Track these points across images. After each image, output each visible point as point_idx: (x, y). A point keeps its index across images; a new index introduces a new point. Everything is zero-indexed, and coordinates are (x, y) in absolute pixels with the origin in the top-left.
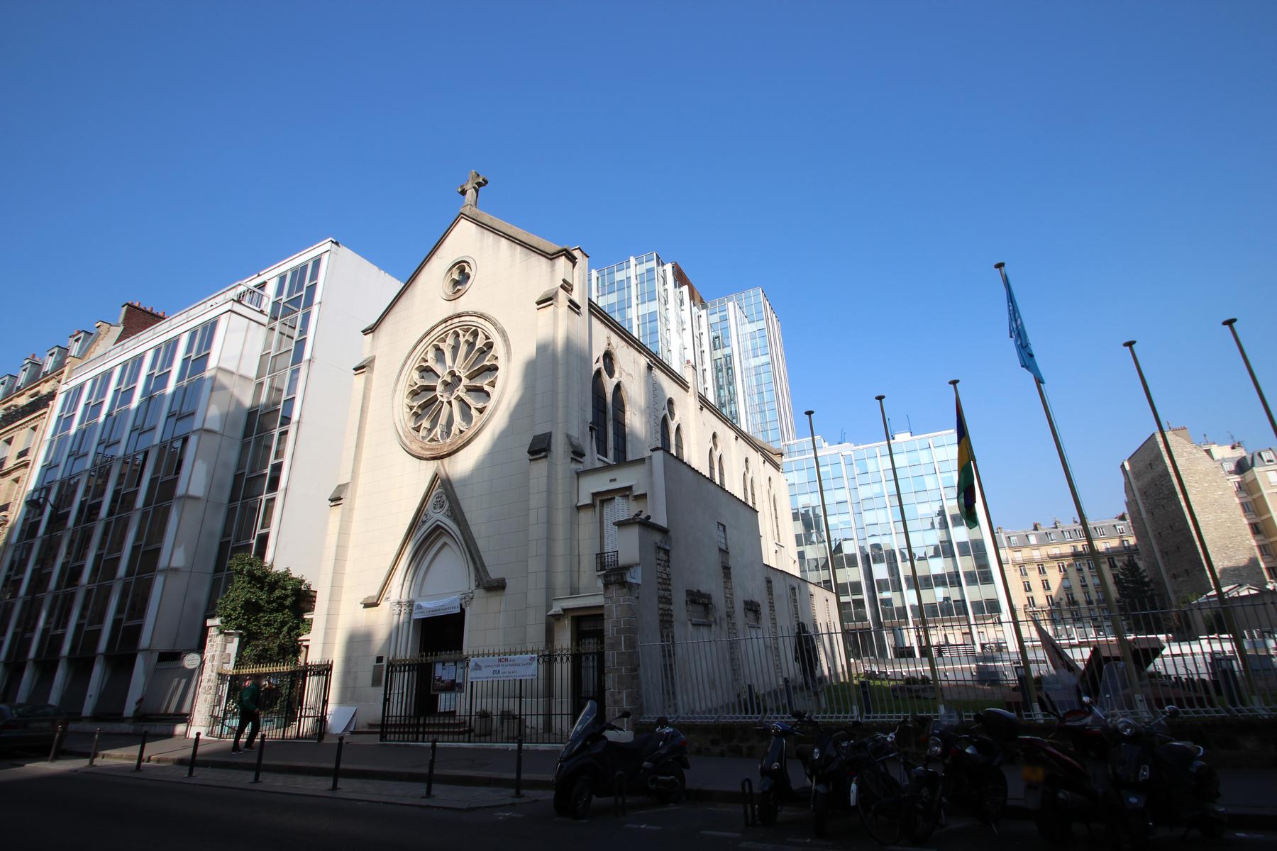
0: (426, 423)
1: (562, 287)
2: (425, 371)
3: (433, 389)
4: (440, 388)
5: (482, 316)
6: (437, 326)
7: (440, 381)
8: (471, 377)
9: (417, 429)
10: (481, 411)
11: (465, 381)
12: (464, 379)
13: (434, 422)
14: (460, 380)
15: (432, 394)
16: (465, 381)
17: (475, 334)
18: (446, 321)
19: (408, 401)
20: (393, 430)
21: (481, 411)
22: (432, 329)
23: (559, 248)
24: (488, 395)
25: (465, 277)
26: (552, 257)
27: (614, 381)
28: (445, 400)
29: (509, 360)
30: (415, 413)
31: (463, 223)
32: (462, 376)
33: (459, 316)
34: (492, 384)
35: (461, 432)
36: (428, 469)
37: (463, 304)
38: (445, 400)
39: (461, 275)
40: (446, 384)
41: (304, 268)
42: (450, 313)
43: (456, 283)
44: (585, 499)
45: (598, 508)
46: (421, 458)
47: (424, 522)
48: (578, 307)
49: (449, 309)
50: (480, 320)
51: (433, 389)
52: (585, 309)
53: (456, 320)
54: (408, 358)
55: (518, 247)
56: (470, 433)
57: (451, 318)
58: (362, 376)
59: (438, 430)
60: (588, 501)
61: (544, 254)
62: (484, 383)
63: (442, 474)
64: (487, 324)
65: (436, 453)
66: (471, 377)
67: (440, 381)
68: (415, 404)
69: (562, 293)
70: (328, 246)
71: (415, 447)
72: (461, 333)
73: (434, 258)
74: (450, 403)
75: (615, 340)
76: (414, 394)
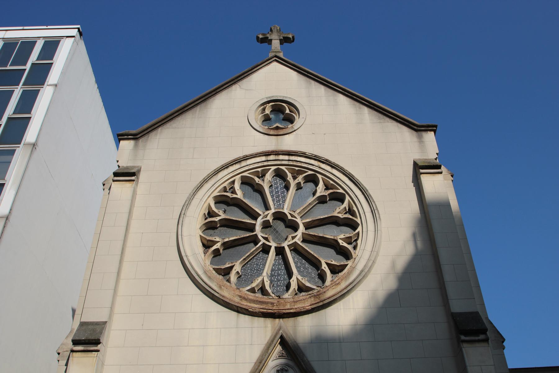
3: (252, 228)
4: (258, 228)
5: (327, 162)
7: (260, 220)
8: (308, 226)
9: (226, 273)
11: (302, 229)
13: (251, 270)
14: (294, 227)
16: (302, 229)
21: (335, 270)
22: (246, 158)
28: (273, 245)
30: (216, 253)
31: (275, 66)
32: (299, 220)
33: (289, 153)
34: (353, 241)
35: (301, 289)
36: (262, 331)
37: (288, 142)
38: (273, 245)
39: (279, 114)
40: (266, 225)
41: (29, 45)
43: (267, 119)
53: (286, 157)
54: (205, 181)
55: (366, 110)
57: (277, 153)
58: (128, 184)
62: (340, 235)
66: (308, 226)
70: (75, 32)
74: (280, 251)
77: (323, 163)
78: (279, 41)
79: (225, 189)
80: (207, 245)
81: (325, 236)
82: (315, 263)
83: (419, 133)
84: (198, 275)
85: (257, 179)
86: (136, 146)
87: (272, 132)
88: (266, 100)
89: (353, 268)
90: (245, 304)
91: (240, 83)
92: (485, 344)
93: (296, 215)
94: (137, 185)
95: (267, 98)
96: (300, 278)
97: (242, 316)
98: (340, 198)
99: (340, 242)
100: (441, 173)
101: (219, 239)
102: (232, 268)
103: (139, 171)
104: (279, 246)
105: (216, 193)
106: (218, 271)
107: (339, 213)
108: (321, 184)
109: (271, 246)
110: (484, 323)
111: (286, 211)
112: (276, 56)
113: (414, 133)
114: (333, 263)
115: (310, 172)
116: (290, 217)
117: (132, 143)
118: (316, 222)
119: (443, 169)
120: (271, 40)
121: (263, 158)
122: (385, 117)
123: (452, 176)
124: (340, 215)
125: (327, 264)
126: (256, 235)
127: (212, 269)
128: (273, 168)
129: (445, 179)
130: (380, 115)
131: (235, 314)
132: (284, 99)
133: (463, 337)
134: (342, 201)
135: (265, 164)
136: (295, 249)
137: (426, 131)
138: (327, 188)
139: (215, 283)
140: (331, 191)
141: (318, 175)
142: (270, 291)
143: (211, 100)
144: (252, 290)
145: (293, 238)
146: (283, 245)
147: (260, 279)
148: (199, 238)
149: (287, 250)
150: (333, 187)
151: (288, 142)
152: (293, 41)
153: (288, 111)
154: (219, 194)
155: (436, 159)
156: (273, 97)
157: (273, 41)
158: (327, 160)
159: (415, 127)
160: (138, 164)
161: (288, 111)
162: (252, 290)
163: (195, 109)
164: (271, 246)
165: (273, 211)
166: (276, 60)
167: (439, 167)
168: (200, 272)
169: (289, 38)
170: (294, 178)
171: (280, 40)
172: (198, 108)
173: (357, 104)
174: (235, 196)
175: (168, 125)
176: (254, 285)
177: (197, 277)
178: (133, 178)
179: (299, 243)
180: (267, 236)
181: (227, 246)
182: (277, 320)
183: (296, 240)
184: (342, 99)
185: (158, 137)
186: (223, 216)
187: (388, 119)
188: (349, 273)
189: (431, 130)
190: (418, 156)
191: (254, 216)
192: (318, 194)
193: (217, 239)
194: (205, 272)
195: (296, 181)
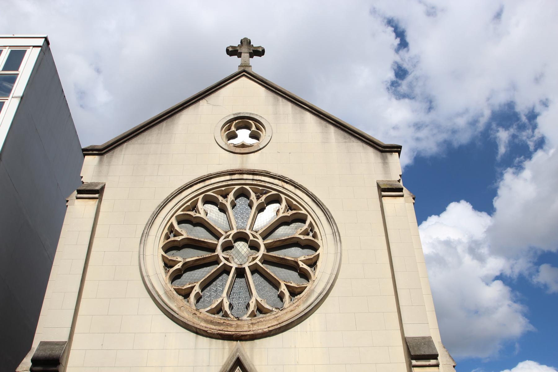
4: (219, 248)
7: (222, 240)
8: (269, 248)
18: (232, 173)
21: (294, 292)
24: (305, 276)
28: (234, 266)
33: (254, 173)
34: (313, 264)
35: (261, 310)
46: (198, 332)
49: (234, 162)
51: (211, 248)
53: (251, 177)
55: (332, 129)
56: (286, 316)
57: (241, 172)
65: (231, 330)
66: (269, 248)
67: (222, 240)
73: (203, 103)
77: (287, 183)
78: (248, 55)
79: (189, 209)
80: (168, 265)
81: (286, 258)
82: (275, 284)
83: (384, 154)
84: (159, 296)
85: (221, 199)
86: (101, 161)
87: (238, 150)
88: (232, 117)
89: (312, 291)
90: (203, 325)
91: (207, 98)
92: (436, 368)
93: (258, 236)
94: (100, 202)
95: (234, 114)
96: (259, 299)
97: (200, 338)
98: (302, 219)
99: (301, 263)
100: (402, 196)
101: (181, 258)
102: (192, 288)
103: (103, 188)
104: (240, 267)
106: (178, 291)
107: (300, 234)
108: (284, 203)
109: (232, 267)
110: (435, 348)
111: (248, 232)
112: (244, 71)
114: (292, 285)
115: (274, 192)
116: (251, 238)
117: (97, 158)
118: (278, 244)
119: (405, 191)
120: (241, 53)
121: (228, 177)
122: (350, 137)
123: (414, 199)
124: (302, 237)
125: (287, 286)
126: (218, 255)
127: (172, 289)
128: (237, 187)
129: (406, 202)
130: (346, 134)
131: (193, 335)
132: (251, 116)
133: (414, 362)
134: (304, 221)
135: (230, 183)
137: (391, 152)
138: (290, 207)
139: (176, 304)
140: (294, 212)
141: (281, 195)
142: (229, 312)
143: (177, 115)
144: (212, 312)
145: (254, 259)
146: (243, 266)
147: (219, 301)
148: (160, 258)
149: (248, 271)
150: (296, 208)
151: (253, 162)
152: (263, 54)
153: (254, 128)
154: (182, 213)
155: (399, 181)
156: (239, 113)
157: (243, 55)
158: (291, 181)
159: (380, 148)
160: (102, 180)
161: (254, 128)
162: (212, 312)
163: (161, 124)
164: (232, 267)
165: (235, 231)
166: (244, 75)
167: (401, 190)
168: (161, 293)
169: (259, 51)
170: (258, 198)
171: (250, 53)
172: (164, 124)
173: (324, 123)
174: (198, 215)
175: (134, 140)
176: (214, 306)
177: (157, 298)
178: (97, 196)
179: (260, 264)
180: (228, 257)
181: (190, 267)
182: (235, 342)
183: (257, 261)
184: (309, 117)
185: (123, 153)
186: (185, 236)
187: (353, 139)
188: (309, 295)
190: (381, 177)
191: (217, 236)
192: (281, 215)
193: (179, 259)
194: (166, 293)
195: (260, 201)
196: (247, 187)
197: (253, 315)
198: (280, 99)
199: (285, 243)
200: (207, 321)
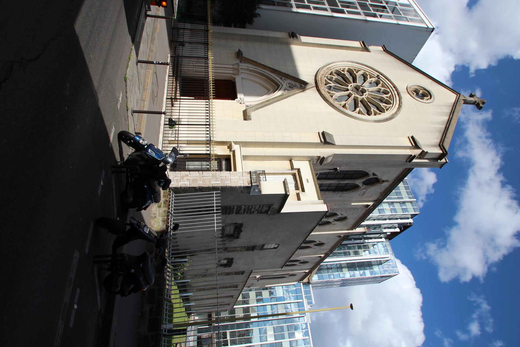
0: (335, 77)
1: (423, 151)
2: (365, 77)
5: (400, 106)
6: (391, 83)
10: (344, 106)
12: (362, 97)
13: (336, 81)
15: (351, 79)
17: (387, 102)
19: (347, 68)
20: (331, 62)
21: (344, 106)
23: (447, 150)
25: (423, 96)
26: (441, 145)
27: (361, 185)
29: (376, 121)
32: (364, 96)
35: (332, 96)
37: (406, 98)
42: (400, 90)
44: (297, 164)
45: (291, 172)
46: (316, 76)
47: (281, 78)
48: (410, 161)
49: (402, 88)
50: (397, 106)
51: (355, 80)
52: (408, 166)
55: (444, 126)
56: (331, 100)
59: (332, 84)
60: (295, 167)
61: (442, 140)
63: (308, 87)
64: (395, 109)
68: (346, 73)
69: (419, 151)
71: (322, 72)
72: (389, 95)
74: (348, 90)
75: (385, 185)
76: (350, 72)
105: (367, 73)
106: (332, 72)
111: (367, 93)
113: (438, 144)
118: (365, 104)
124: (372, 110)
136: (349, 96)
137: (441, 149)
173: (445, 123)
179: (353, 96)
189: (443, 151)
196: (390, 93)
197: (329, 93)
198: (451, 108)
199: (367, 106)
200: (321, 79)
